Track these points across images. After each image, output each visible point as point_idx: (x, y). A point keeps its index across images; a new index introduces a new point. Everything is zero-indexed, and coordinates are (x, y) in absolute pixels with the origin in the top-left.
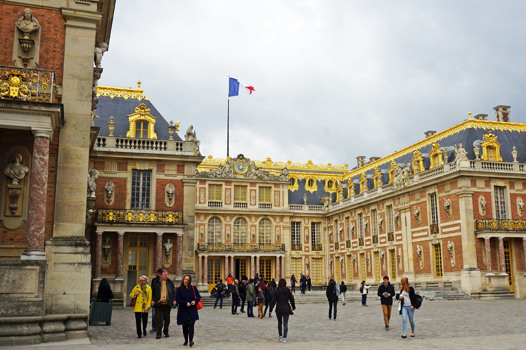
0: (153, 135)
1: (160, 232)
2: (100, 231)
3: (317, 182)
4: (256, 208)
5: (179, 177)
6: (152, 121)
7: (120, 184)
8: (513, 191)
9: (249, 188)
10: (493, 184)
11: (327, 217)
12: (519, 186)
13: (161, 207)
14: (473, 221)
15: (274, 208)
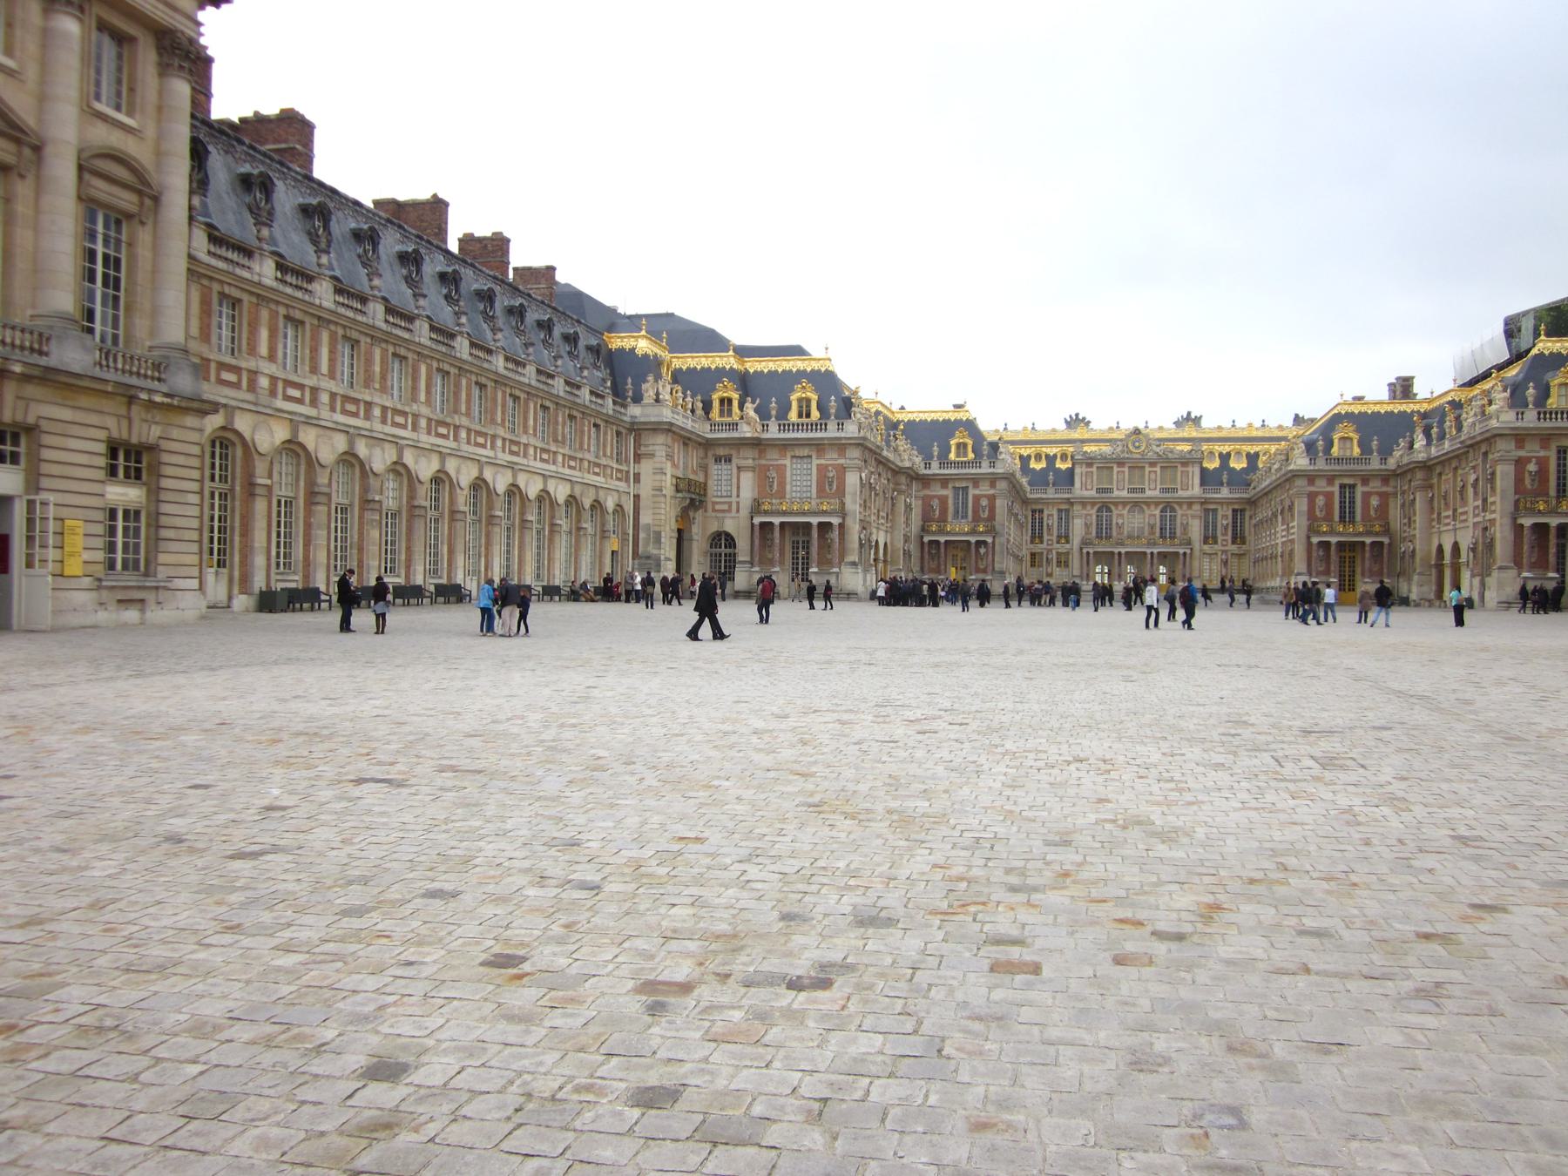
0: (971, 456)
1: (973, 539)
2: (926, 539)
3: (1248, 455)
4: (1156, 493)
5: (992, 492)
6: (970, 442)
7: (943, 501)
8: (1366, 489)
9: (1148, 469)
10: (1337, 482)
11: (1252, 503)
12: (1375, 485)
13: (977, 518)
14: (1305, 523)
15: (1181, 493)
